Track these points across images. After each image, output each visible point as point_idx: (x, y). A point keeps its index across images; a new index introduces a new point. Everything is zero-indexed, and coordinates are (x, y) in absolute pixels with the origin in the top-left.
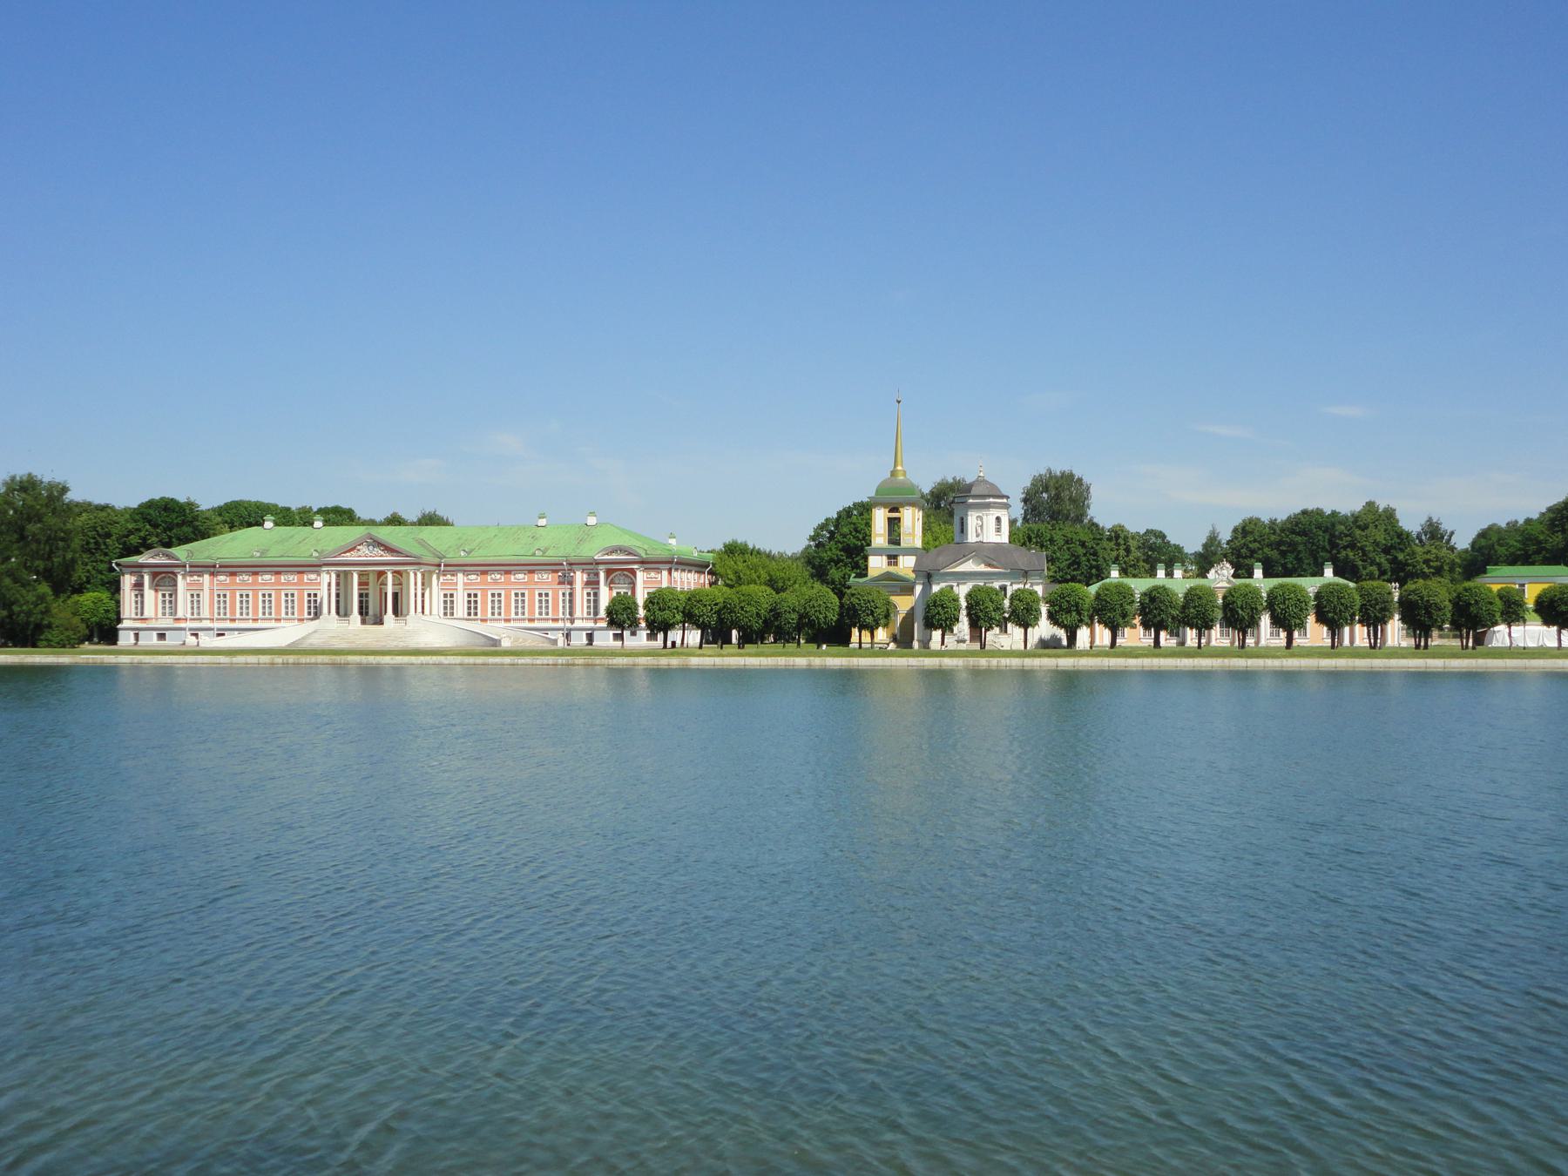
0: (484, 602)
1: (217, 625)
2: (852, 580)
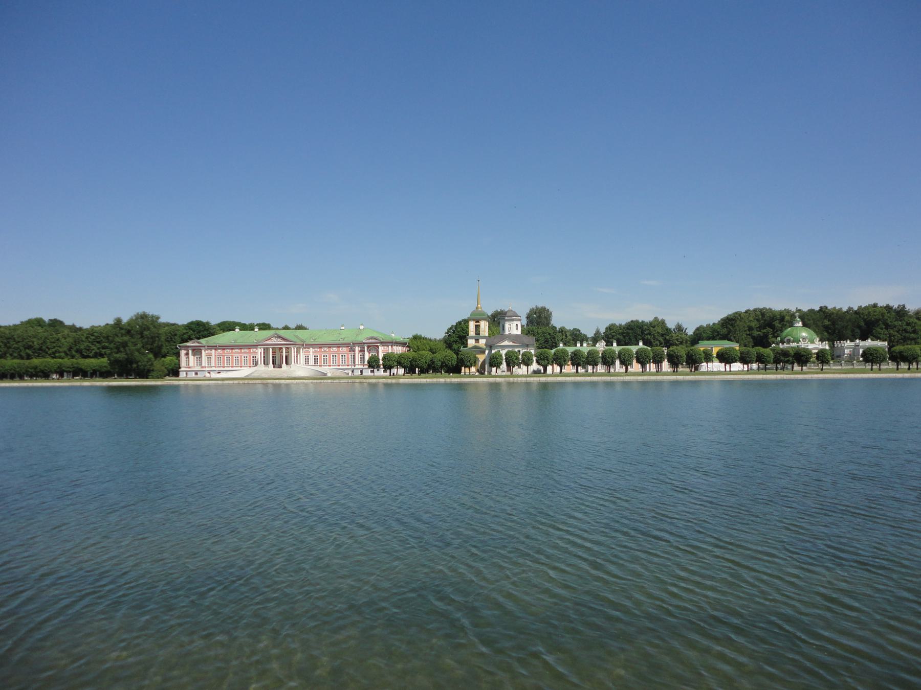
2: (462, 348)
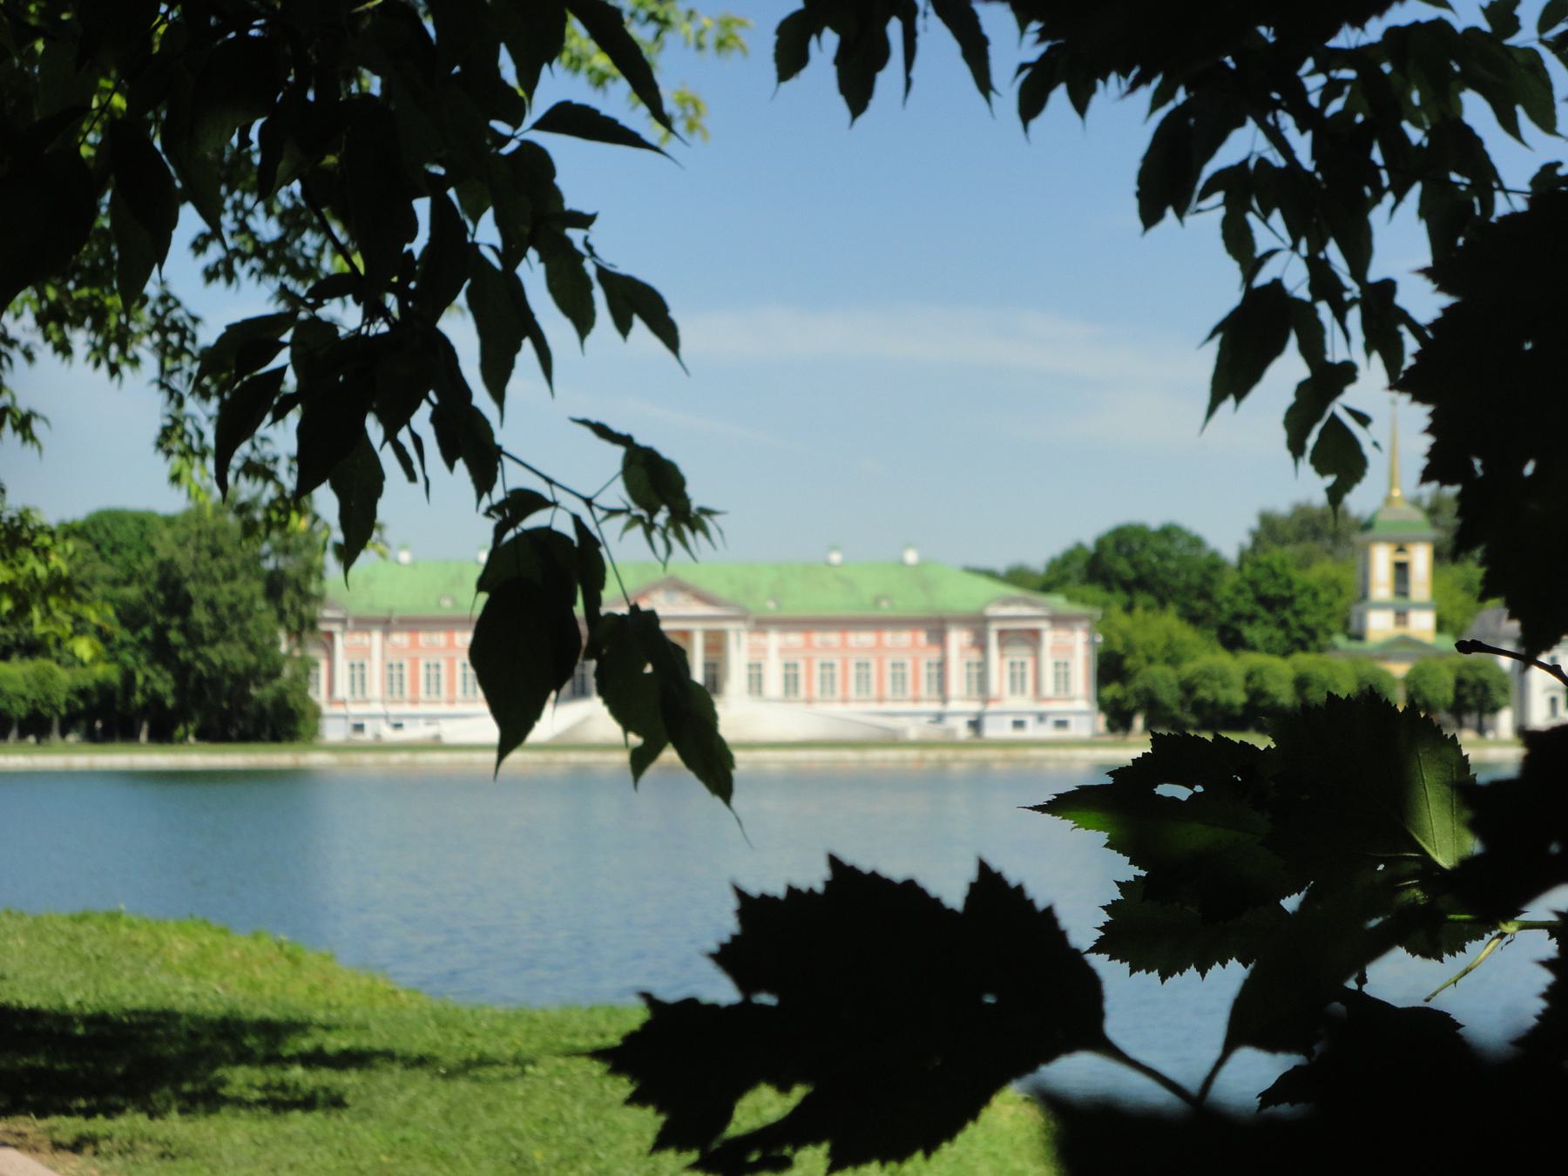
1: (394, 710)
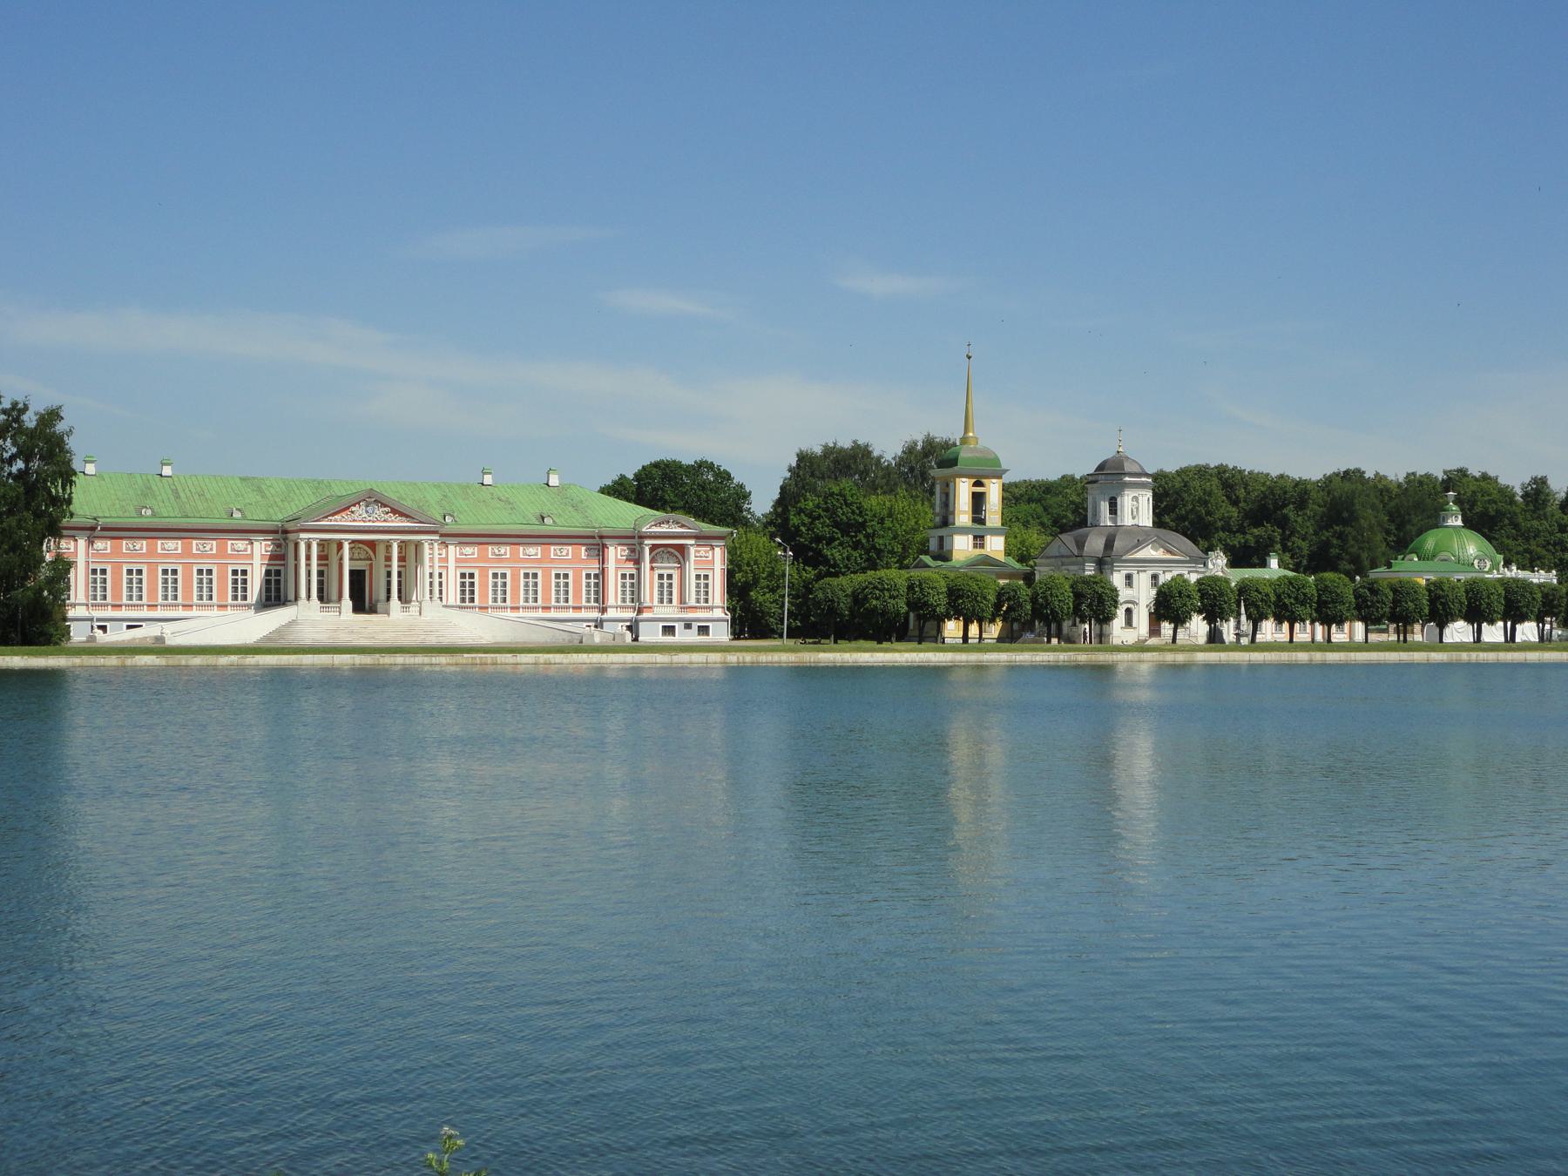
0: (484, 585)
